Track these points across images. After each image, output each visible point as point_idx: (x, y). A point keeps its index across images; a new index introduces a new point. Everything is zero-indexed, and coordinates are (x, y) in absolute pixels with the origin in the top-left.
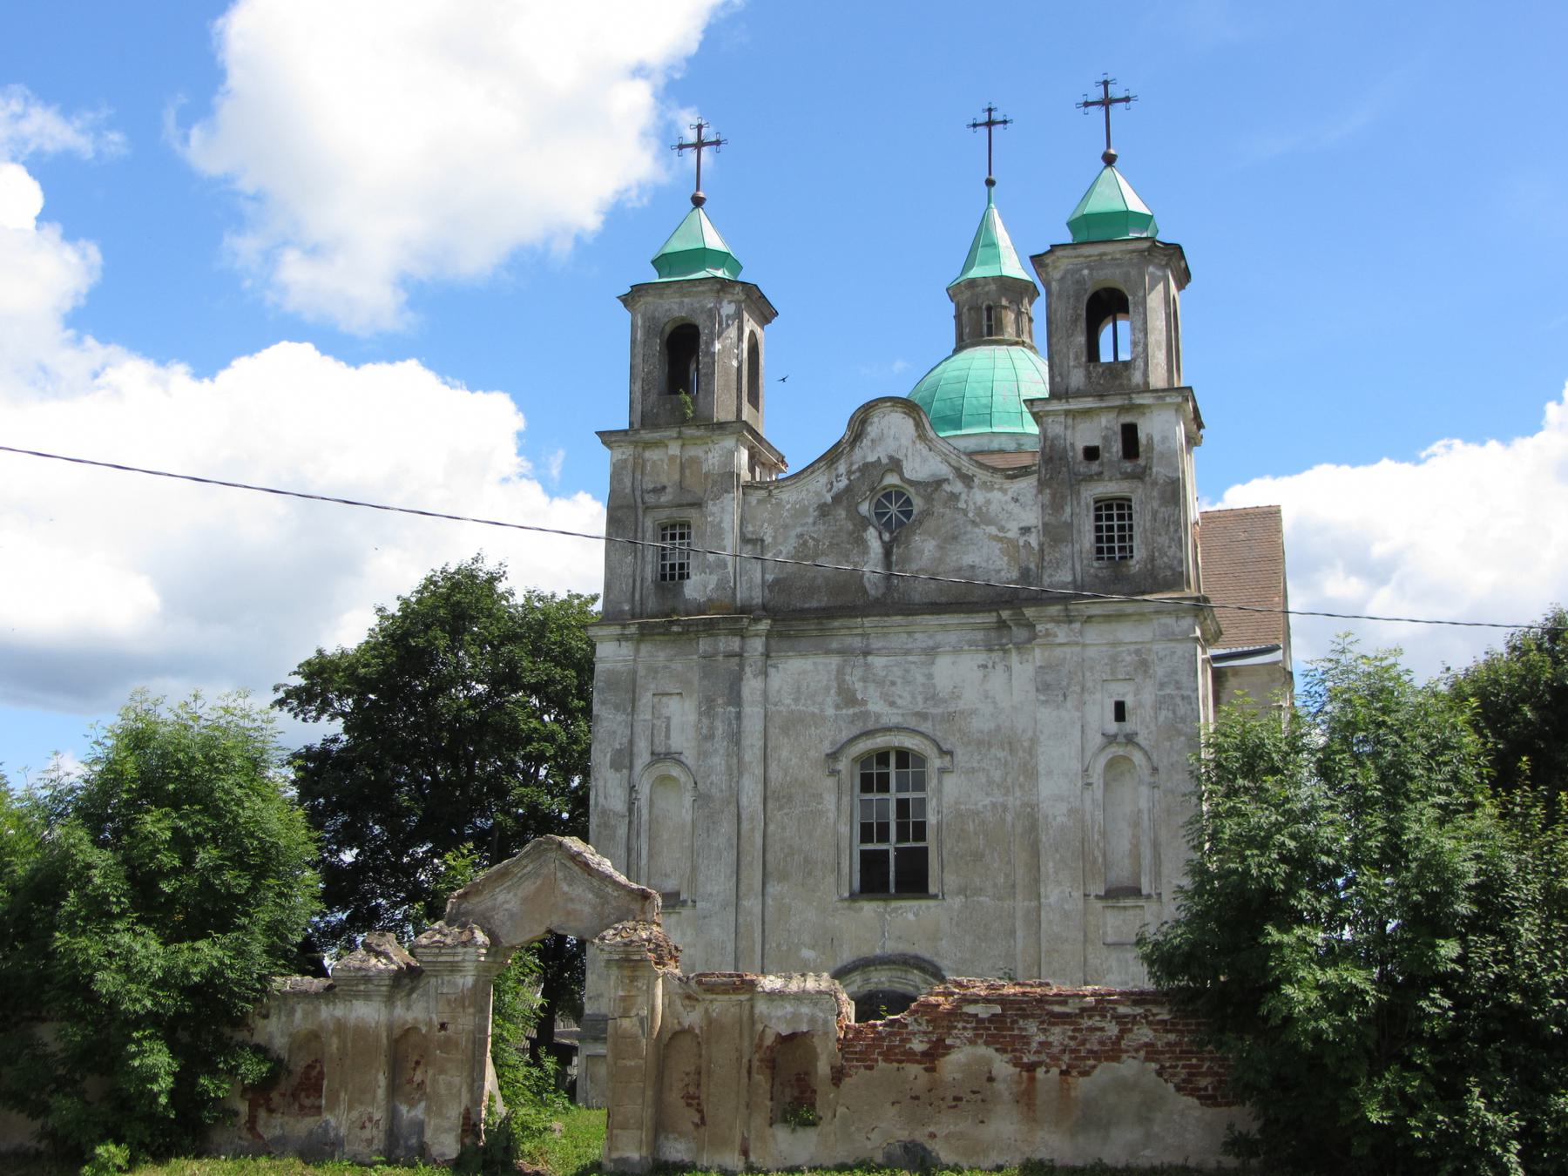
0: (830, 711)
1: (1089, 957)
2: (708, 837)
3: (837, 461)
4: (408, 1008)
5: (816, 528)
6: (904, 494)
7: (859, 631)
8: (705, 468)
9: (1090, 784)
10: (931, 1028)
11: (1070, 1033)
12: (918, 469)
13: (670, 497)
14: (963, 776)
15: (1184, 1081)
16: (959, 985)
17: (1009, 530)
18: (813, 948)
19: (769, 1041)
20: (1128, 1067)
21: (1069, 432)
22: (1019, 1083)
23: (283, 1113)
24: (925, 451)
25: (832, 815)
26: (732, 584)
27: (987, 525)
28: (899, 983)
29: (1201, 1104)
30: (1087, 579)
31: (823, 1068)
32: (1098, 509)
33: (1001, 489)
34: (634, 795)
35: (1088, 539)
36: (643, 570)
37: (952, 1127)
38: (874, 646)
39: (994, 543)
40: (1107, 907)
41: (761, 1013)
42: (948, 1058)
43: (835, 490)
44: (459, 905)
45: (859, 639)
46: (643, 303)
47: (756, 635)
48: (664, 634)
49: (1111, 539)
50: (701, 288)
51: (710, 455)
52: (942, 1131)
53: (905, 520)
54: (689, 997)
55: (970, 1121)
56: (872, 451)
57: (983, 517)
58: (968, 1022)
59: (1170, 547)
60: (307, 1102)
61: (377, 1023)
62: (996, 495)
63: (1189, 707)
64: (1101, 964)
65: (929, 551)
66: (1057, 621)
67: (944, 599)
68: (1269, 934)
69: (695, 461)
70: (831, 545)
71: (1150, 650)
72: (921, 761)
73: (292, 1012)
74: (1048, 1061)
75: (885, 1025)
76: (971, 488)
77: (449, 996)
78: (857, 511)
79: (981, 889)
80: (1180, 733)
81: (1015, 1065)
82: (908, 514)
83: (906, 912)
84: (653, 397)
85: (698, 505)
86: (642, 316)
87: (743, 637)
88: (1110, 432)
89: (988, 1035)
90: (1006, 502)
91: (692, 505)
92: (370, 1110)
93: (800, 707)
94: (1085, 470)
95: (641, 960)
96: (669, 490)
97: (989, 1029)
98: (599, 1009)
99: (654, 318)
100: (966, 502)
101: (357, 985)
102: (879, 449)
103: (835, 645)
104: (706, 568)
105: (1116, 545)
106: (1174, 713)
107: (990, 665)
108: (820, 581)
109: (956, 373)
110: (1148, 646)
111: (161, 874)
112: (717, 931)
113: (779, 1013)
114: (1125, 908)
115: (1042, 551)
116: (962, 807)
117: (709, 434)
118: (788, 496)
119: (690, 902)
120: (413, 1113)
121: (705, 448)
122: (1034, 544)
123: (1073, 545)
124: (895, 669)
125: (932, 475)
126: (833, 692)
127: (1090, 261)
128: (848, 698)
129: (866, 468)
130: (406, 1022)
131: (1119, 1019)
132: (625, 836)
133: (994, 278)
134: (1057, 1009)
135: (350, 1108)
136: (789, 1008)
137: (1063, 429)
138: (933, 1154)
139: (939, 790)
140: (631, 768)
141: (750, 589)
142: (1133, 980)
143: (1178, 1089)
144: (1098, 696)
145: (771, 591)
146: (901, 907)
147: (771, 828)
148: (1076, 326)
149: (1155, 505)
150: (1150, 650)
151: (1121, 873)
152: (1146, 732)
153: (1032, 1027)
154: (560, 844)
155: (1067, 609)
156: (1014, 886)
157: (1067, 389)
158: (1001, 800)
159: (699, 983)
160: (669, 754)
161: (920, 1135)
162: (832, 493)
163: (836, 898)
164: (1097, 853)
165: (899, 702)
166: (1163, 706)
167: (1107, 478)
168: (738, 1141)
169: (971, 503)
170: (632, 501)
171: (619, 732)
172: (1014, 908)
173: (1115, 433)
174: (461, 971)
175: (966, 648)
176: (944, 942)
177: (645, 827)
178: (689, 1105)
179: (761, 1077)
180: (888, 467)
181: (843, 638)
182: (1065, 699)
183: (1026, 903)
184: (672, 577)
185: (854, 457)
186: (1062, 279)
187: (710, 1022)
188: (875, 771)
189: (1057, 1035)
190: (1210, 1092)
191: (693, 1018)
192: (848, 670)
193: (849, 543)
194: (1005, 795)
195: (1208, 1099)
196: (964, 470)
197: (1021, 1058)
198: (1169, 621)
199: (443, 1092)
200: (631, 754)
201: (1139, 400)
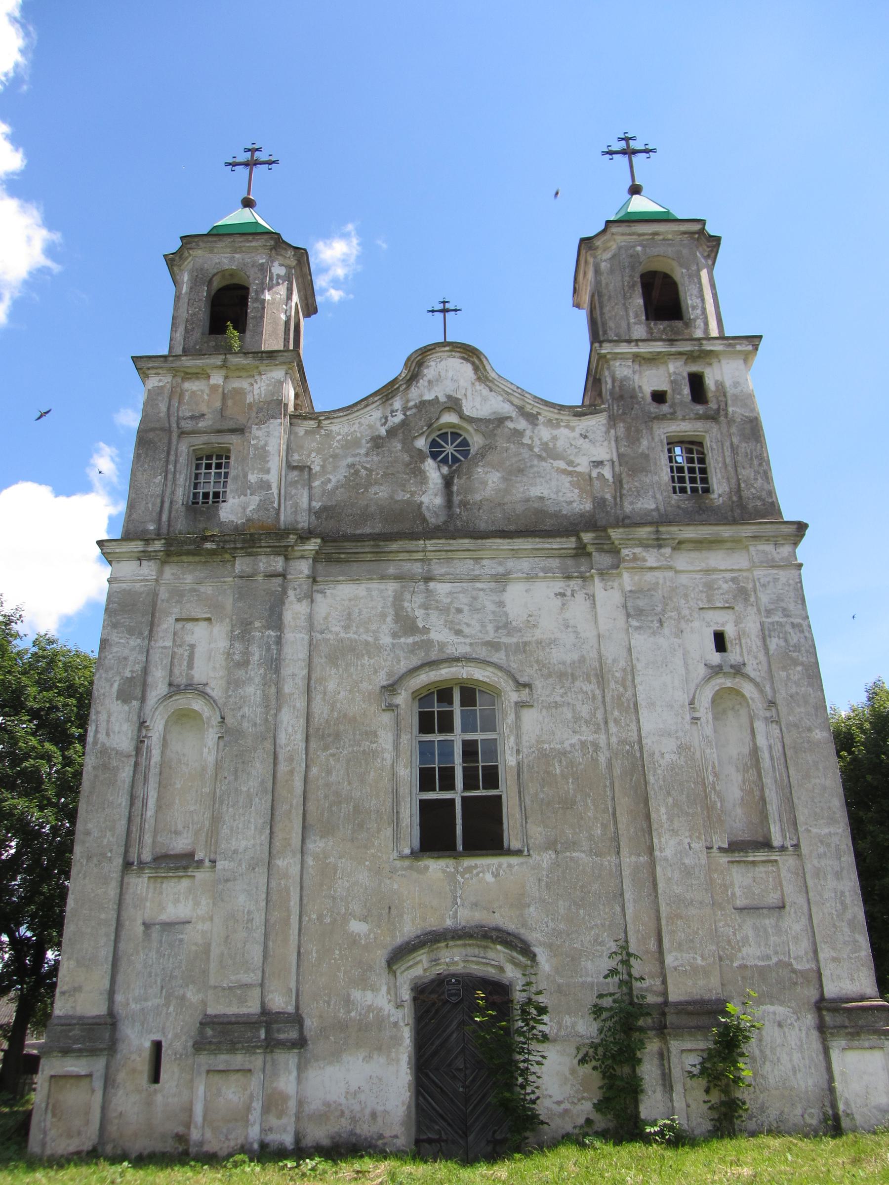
0: (386, 640)
2: (236, 779)
3: (392, 397)
5: (369, 459)
7: (420, 556)
8: (249, 399)
12: (479, 407)
13: (210, 423)
14: (544, 711)
17: (579, 464)
18: (364, 919)
21: (636, 377)
24: (485, 392)
25: (388, 756)
26: (276, 505)
27: (554, 460)
28: (478, 963)
33: (567, 427)
34: (144, 732)
36: (173, 493)
39: (563, 476)
40: (732, 862)
43: (390, 424)
45: (419, 564)
47: (302, 557)
50: (254, 244)
51: (256, 386)
53: (462, 459)
56: (429, 390)
57: (550, 452)
59: (756, 479)
62: (563, 432)
63: (802, 635)
64: (735, 934)
65: (493, 482)
66: (646, 547)
67: (512, 528)
69: (240, 393)
70: (385, 475)
71: (747, 578)
72: (493, 693)
76: (537, 425)
79: (574, 843)
80: (795, 662)
82: (466, 453)
83: (483, 872)
84: (197, 335)
85: (240, 431)
86: (191, 272)
87: (287, 559)
88: (679, 378)
90: (575, 439)
91: (233, 431)
93: (351, 635)
94: (657, 410)
98: (74, 1008)
99: (202, 269)
100: (531, 438)
102: (436, 388)
103: (391, 570)
104: (246, 489)
106: (786, 641)
107: (569, 593)
108: (373, 509)
112: (242, 899)
116: (546, 746)
117: (257, 363)
118: (339, 429)
119: (207, 863)
124: (461, 595)
125: (494, 413)
126: (389, 619)
127: (643, 240)
129: (422, 405)
132: (128, 781)
137: (631, 372)
140: (143, 699)
141: (295, 513)
142: (776, 953)
144: (696, 624)
145: (318, 518)
146: (476, 866)
147: (314, 771)
148: (634, 290)
149: (735, 440)
152: (755, 663)
155: (657, 532)
158: (591, 738)
160: (190, 685)
162: (386, 427)
163: (395, 855)
165: (466, 630)
166: (772, 634)
167: (680, 417)
169: (536, 439)
170: (167, 425)
171: (131, 658)
173: (684, 378)
175: (541, 574)
176: (532, 909)
180: (447, 405)
181: (401, 563)
182: (662, 625)
183: (633, 859)
185: (410, 395)
188: (436, 709)
192: (407, 596)
193: (404, 473)
194: (595, 732)
196: (528, 408)
198: (769, 548)
200: (144, 685)
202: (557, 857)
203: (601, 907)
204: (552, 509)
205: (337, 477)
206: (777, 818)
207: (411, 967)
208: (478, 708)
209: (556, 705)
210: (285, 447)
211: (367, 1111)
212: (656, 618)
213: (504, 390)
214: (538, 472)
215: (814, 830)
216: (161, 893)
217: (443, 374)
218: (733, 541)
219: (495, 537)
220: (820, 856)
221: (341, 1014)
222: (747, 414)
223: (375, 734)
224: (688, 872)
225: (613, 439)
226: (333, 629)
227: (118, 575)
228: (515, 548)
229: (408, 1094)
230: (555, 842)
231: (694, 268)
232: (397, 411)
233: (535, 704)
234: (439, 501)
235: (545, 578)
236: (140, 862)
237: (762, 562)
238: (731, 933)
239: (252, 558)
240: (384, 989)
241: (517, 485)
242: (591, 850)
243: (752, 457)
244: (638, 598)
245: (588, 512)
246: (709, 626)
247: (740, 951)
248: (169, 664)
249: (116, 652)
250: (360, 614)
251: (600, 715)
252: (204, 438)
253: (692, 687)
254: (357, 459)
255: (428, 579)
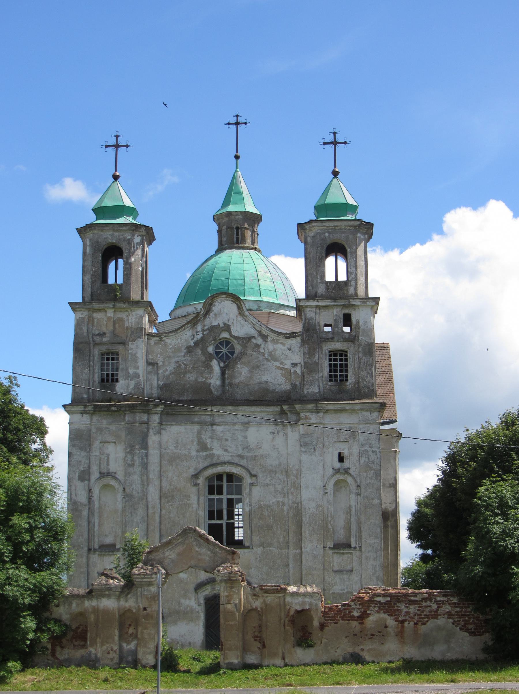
0: (194, 453)
1: (326, 577)
3: (197, 324)
4: (126, 601)
5: (185, 359)
6: (230, 343)
7: (209, 413)
8: (126, 324)
9: (326, 493)
10: (361, 607)
11: (417, 608)
12: (239, 331)
13: (109, 339)
14: (262, 488)
15: (463, 626)
16: (371, 589)
17: (286, 364)
19: (292, 613)
20: (441, 621)
21: (317, 316)
22: (397, 628)
23: (68, 648)
24: (243, 322)
25: (195, 506)
26: (142, 386)
29: (470, 635)
30: (325, 391)
31: (316, 623)
32: (330, 355)
33: (281, 343)
34: (91, 494)
35: (326, 371)
36: (93, 377)
37: (370, 646)
38: (217, 421)
39: (278, 370)
41: (288, 601)
42: (368, 619)
43: (195, 339)
44: (148, 556)
45: (208, 417)
46: (90, 234)
47: (156, 413)
48: (106, 411)
49: (336, 371)
50: (124, 228)
51: (130, 318)
52: (366, 648)
53: (231, 356)
54: (255, 595)
55: (377, 643)
56: (215, 320)
57: (273, 357)
58: (376, 604)
59: (367, 377)
60: (76, 643)
61: (113, 608)
62: (279, 346)
63: (376, 456)
64: (332, 581)
65: (245, 373)
66: (311, 412)
67: (252, 398)
68: (514, 569)
69: (121, 320)
71: (356, 428)
72: (240, 479)
73: (71, 604)
74: (409, 619)
75: (341, 606)
76: (267, 342)
77: (148, 596)
78: (207, 351)
79: (271, 544)
80: (371, 469)
81: (396, 621)
82: (232, 353)
85: (123, 343)
87: (149, 414)
88: (338, 318)
89: (384, 609)
90: (285, 350)
91: (119, 343)
92: (112, 645)
95: (236, 580)
96: (107, 335)
97: (385, 607)
99: (97, 242)
100: (264, 349)
101: (105, 591)
102: (218, 319)
103: (196, 419)
104: (127, 377)
105: (338, 374)
106: (368, 459)
107: (276, 432)
109: (223, 265)
110: (355, 426)
111: (23, 543)
113: (296, 601)
114: (343, 554)
115: (303, 376)
116: (262, 503)
117: (130, 307)
120: (129, 647)
121: (126, 313)
122: (299, 372)
123: (319, 374)
124: (228, 433)
125: (247, 334)
126: (195, 443)
127: (329, 229)
128: (203, 447)
130: (125, 607)
131: (437, 602)
132: (87, 516)
133: (241, 213)
134: (412, 598)
135: (102, 645)
136: (300, 599)
137: (314, 315)
138: (363, 657)
139: (250, 495)
140: (89, 480)
141: (151, 389)
142: (347, 588)
143: (461, 629)
144: (331, 450)
145: (162, 390)
147: (164, 512)
149: (360, 356)
150: (356, 428)
151: (341, 536)
152: (354, 468)
153: (402, 606)
154: (195, 530)
155: (317, 406)
156: (288, 542)
157: (316, 293)
158: (281, 500)
159: (261, 589)
161: (357, 650)
162: (194, 341)
164: (329, 526)
165: (230, 449)
166: (363, 455)
167: (336, 341)
168: (280, 654)
169: (266, 350)
170: (88, 340)
172: (288, 553)
173: (340, 318)
174: (153, 585)
175: (264, 423)
176: (253, 570)
177: (96, 511)
178: (255, 640)
179: (289, 628)
181: (201, 416)
182: (315, 450)
183: (294, 551)
184: (108, 381)
186: (314, 237)
187: (266, 605)
188: (216, 484)
189: (412, 609)
190: (473, 630)
191: (257, 604)
192: (203, 432)
195: (472, 633)
196: (263, 332)
197: (398, 618)
198: (367, 414)
199: (146, 637)
200: (89, 474)
201: (353, 302)
202: (264, 550)
203: (280, 569)
204: (272, 388)
205: (170, 368)
206: (354, 536)
207: (204, 591)
208: (234, 484)
209: (267, 485)
210: (145, 353)
211: (188, 642)
212: (313, 447)
213: (251, 322)
214: (266, 368)
215: (368, 541)
216: (103, 561)
217: (222, 310)
218: (352, 410)
219: (244, 405)
220: (369, 552)
221: (177, 608)
222: (368, 341)
223: (189, 496)
224: (315, 557)
225: (302, 352)
226: (170, 448)
227: (73, 421)
228: (253, 410)
229: (203, 636)
230: (264, 543)
231: (354, 248)
232: (199, 332)
233: (258, 484)
234: (219, 382)
235: (266, 425)
236: (94, 549)
237: (363, 421)
238: (330, 580)
239: (133, 414)
240: (194, 599)
241: (256, 375)
242: (278, 547)
243: (367, 365)
244: (306, 437)
245: (288, 390)
246: (337, 450)
247: (333, 587)
248: (99, 464)
249: (76, 458)
250: (182, 441)
251: (286, 490)
252: (106, 346)
253: (326, 478)
254: (180, 358)
255: (213, 424)
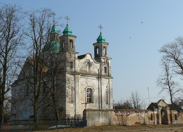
128: (87, 83)
205: (81, 66)
